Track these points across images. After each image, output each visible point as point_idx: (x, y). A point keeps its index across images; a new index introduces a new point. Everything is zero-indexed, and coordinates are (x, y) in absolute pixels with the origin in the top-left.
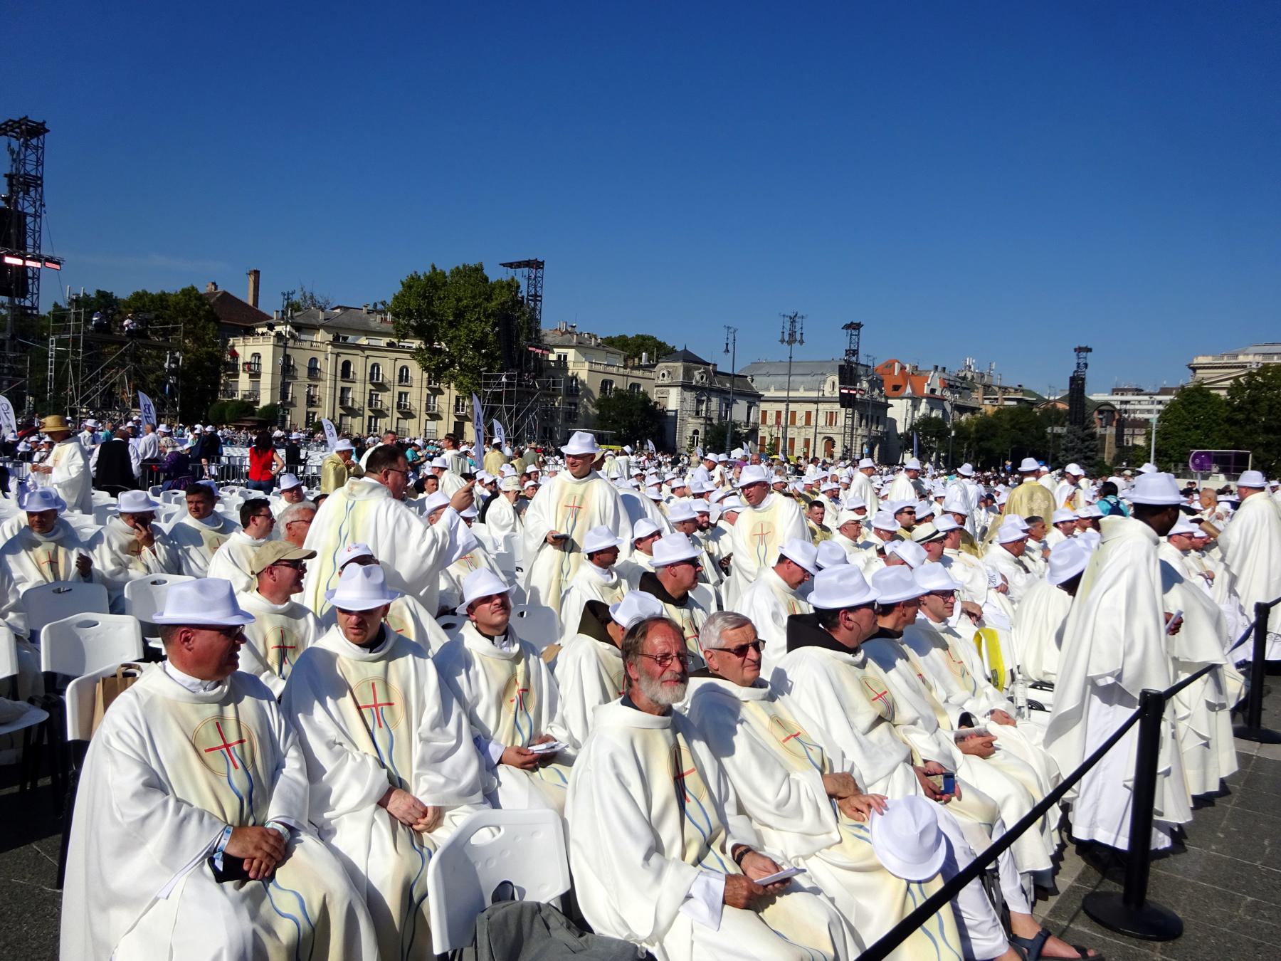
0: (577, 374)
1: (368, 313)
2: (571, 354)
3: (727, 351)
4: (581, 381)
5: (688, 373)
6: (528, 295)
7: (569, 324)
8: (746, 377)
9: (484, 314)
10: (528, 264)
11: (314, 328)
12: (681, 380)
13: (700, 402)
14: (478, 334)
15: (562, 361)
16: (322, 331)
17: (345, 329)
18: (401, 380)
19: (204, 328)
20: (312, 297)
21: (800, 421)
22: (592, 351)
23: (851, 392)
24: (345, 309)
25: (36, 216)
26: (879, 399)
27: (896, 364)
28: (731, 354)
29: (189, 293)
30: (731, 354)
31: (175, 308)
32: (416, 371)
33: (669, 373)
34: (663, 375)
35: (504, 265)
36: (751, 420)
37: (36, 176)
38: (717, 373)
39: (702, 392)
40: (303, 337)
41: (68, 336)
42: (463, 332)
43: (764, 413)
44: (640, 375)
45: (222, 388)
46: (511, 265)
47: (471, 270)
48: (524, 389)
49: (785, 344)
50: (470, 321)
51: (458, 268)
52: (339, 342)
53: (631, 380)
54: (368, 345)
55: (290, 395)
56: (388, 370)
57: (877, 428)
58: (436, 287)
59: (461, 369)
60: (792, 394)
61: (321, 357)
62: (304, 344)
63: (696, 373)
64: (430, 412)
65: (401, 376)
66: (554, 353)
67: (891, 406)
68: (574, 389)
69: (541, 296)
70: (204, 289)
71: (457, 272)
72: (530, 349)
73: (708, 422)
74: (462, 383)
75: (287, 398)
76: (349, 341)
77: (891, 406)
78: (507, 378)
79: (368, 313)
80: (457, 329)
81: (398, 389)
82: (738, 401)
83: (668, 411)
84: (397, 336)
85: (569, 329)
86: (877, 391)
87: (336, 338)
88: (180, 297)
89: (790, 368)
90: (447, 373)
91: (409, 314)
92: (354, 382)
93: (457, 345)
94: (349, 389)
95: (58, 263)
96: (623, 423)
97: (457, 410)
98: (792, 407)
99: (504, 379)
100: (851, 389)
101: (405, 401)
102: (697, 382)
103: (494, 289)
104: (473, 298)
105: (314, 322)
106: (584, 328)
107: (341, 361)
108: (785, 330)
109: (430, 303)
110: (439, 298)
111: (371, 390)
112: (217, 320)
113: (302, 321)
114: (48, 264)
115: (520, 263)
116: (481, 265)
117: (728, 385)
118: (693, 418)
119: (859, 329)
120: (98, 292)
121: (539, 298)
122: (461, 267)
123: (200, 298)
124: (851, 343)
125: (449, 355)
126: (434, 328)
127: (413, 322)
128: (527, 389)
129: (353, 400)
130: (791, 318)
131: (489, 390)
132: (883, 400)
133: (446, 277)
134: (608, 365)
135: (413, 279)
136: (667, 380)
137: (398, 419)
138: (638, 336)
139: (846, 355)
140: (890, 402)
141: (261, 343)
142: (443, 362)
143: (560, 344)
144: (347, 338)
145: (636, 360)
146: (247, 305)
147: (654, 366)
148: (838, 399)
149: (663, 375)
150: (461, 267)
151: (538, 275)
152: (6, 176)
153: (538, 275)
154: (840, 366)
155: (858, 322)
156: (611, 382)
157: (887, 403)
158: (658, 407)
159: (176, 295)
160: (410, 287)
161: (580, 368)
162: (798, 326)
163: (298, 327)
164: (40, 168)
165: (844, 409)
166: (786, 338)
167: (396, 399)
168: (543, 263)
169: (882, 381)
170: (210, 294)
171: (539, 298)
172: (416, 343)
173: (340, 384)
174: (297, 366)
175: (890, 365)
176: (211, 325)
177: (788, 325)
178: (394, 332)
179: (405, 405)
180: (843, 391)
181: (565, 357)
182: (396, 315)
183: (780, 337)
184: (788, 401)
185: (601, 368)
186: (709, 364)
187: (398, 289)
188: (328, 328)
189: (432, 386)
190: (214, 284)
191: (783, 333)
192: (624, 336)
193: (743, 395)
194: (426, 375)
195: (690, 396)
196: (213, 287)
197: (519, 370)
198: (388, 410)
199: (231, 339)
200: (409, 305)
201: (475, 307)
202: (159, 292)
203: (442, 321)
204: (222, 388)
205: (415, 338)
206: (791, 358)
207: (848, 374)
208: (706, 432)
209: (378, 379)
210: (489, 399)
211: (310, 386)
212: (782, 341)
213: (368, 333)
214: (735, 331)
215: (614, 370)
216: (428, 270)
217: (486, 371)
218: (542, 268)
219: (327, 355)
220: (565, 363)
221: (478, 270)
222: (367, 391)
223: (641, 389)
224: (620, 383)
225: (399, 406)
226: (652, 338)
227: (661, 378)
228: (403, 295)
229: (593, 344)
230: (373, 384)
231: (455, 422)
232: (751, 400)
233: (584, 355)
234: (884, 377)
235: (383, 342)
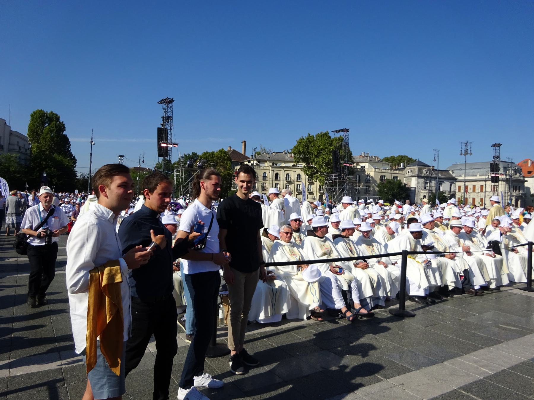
0: (369, 174)
1: (285, 154)
2: (367, 165)
4: (371, 177)
5: (420, 171)
7: (366, 153)
8: (449, 171)
9: (329, 151)
10: (343, 130)
11: (265, 161)
12: (417, 174)
13: (426, 183)
14: (327, 159)
15: (363, 168)
16: (268, 162)
17: (276, 160)
18: (297, 179)
19: (227, 164)
20: (264, 149)
21: (470, 190)
22: (376, 164)
23: (496, 175)
24: (277, 153)
25: (171, 129)
26: (520, 178)
27: (529, 161)
28: (436, 162)
29: (221, 151)
30: (436, 162)
31: (217, 157)
32: (303, 176)
33: (411, 171)
34: (409, 172)
35: (333, 132)
36: (452, 190)
37: (171, 117)
38: (434, 170)
39: (427, 179)
40: (261, 165)
41: (179, 169)
42: (321, 159)
43: (459, 187)
44: (380, 171)
45: (233, 185)
46: (336, 131)
47: (324, 134)
48: (341, 180)
49: (463, 155)
50: (323, 154)
51: (318, 134)
52: (274, 165)
53: (393, 175)
54: (285, 166)
55: (256, 187)
56: (293, 176)
57: (519, 191)
58: (310, 142)
59: (321, 174)
60: (467, 178)
61: (267, 172)
62: (261, 167)
63: (424, 170)
64: (309, 191)
65: (298, 178)
66: (359, 165)
67: (527, 181)
68: (368, 180)
70: (226, 149)
71: (318, 135)
72: (344, 164)
73: (430, 192)
74: (321, 179)
75: (255, 188)
76: (278, 165)
77: (527, 181)
78: (334, 176)
79: (285, 154)
80: (318, 158)
81: (297, 183)
82: (445, 182)
83: (411, 188)
84: (295, 162)
85: (366, 155)
86: (518, 174)
87: (273, 164)
88: (218, 153)
89: (466, 166)
90: (315, 175)
91: (300, 153)
92: (280, 181)
93: (319, 164)
94: (278, 184)
95: (177, 145)
96: (390, 193)
97: (320, 190)
98: (467, 184)
99: (333, 177)
100: (496, 174)
101: (299, 188)
102: (425, 174)
103: (333, 141)
104: (325, 145)
105: (265, 159)
106: (372, 154)
107: (275, 173)
108: (462, 149)
109: (308, 149)
110: (311, 146)
111: (286, 184)
112: (231, 160)
113: (260, 159)
114: (174, 145)
115: (339, 130)
116: (328, 131)
117: (440, 175)
118: (423, 190)
119: (499, 146)
120: (193, 153)
123: (225, 152)
124: (495, 153)
125: (316, 168)
126: (310, 158)
127: (301, 156)
128: (343, 181)
129: (279, 188)
130: (465, 144)
131: (328, 182)
132: (522, 178)
133: (314, 138)
134: (383, 169)
135: (301, 139)
136: (410, 174)
137: (297, 195)
138: (399, 156)
139: (494, 158)
140: (526, 179)
142: (313, 171)
143: (362, 161)
144: (277, 164)
145: (397, 166)
146: (241, 154)
148: (490, 179)
149: (409, 172)
151: (347, 134)
152: (162, 117)
153: (347, 134)
154: (491, 164)
155: (499, 143)
156: (384, 176)
157: (524, 180)
158: (407, 186)
160: (300, 143)
161: (370, 171)
162: (469, 147)
163: (259, 161)
164: (172, 114)
165: (493, 184)
166: (463, 152)
167: (296, 187)
168: (349, 130)
169: (521, 170)
170: (229, 151)
172: (303, 165)
173: (275, 182)
174: (259, 176)
175: (526, 162)
176: (229, 162)
177: (464, 147)
178: (294, 161)
179: (299, 189)
180: (492, 175)
181: (364, 167)
182: (295, 154)
183: (460, 152)
184: (465, 181)
185: (380, 171)
186: (430, 166)
187: (296, 144)
188: (270, 161)
189: (310, 181)
190: (230, 147)
191: (461, 150)
192: (393, 156)
193: (447, 179)
194: (307, 177)
195: (421, 181)
197: (339, 173)
198: (293, 191)
199: (236, 167)
200: (300, 149)
201: (325, 149)
202: (212, 151)
203: (312, 155)
204: (233, 185)
205: (302, 162)
206: (466, 161)
207: (494, 168)
208: (429, 196)
209: (289, 179)
211: (263, 183)
212: (461, 154)
213: (285, 162)
214: (438, 151)
215: (386, 171)
216: (307, 136)
217: (326, 174)
219: (270, 171)
220: (364, 169)
221: (327, 134)
222: (285, 184)
223: (398, 179)
224: (388, 177)
225: (297, 190)
227: (408, 173)
228: (297, 146)
229: (376, 160)
230: (287, 181)
231: (319, 195)
232: (451, 181)
233: (372, 165)
234: (522, 168)
235: (291, 165)
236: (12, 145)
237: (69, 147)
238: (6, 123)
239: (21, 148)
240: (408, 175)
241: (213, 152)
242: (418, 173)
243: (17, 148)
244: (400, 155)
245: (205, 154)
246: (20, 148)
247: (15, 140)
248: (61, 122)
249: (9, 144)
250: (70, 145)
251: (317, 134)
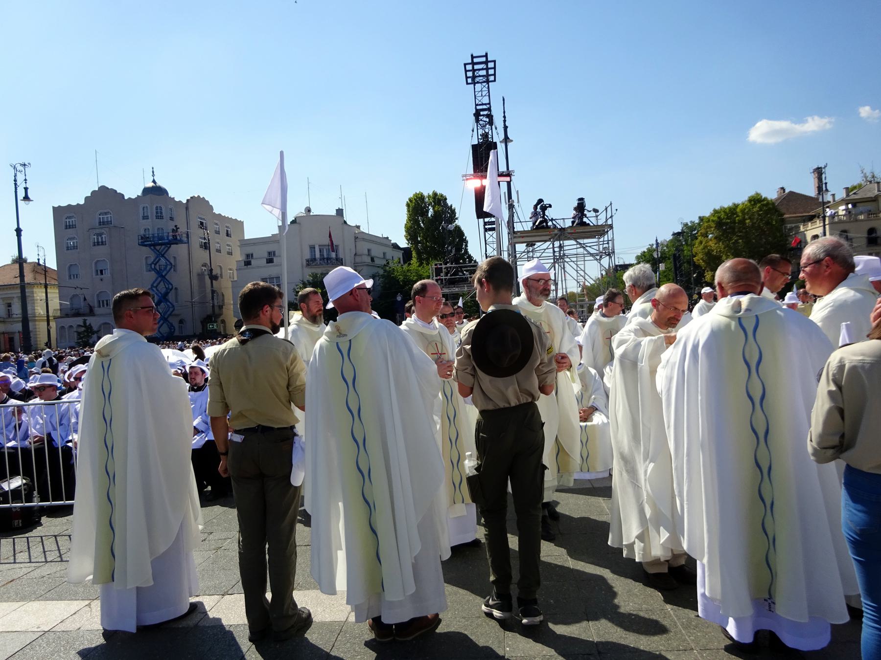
20: (873, 177)
141: (818, 226)
159: (743, 204)
190: (783, 189)
196: (782, 191)
202: (730, 204)
236: (359, 255)
237: (466, 246)
238: (345, 222)
239: (375, 259)
241: (735, 204)
243: (368, 260)
245: (716, 212)
246: (372, 260)
247: (363, 247)
248: (449, 205)
249: (355, 254)
250: (467, 242)
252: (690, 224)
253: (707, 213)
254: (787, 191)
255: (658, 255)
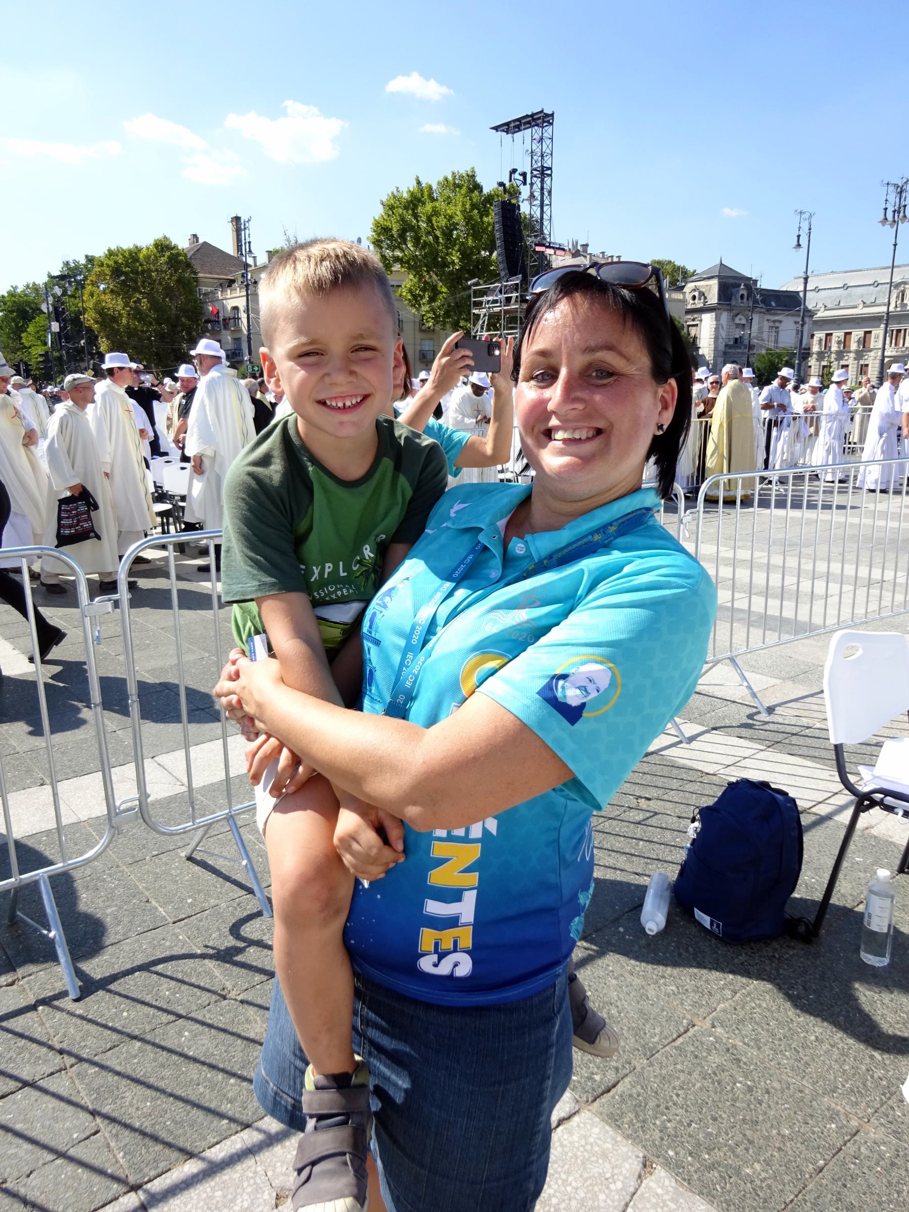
3: (799, 245)
6: (533, 170)
34: (694, 298)
35: (496, 128)
49: (887, 227)
69: (550, 169)
71: (445, 184)
72: (538, 249)
116: (473, 171)
120: (87, 257)
121: (549, 172)
122: (450, 178)
136: (699, 304)
141: (238, 295)
147: (683, 287)
150: (450, 178)
153: (545, 135)
160: (392, 208)
168: (552, 115)
171: (549, 172)
177: (893, 198)
183: (882, 217)
187: (378, 212)
190: (195, 236)
191: (886, 209)
210: (482, 328)
214: (811, 216)
216: (412, 185)
218: (552, 124)
226: (670, 262)
227: (692, 302)
240: (693, 306)
242: (720, 299)
244: (657, 259)
245: (111, 253)
251: (441, 179)
252: (73, 265)
253: (99, 252)
254: (201, 241)
255: (48, 309)
